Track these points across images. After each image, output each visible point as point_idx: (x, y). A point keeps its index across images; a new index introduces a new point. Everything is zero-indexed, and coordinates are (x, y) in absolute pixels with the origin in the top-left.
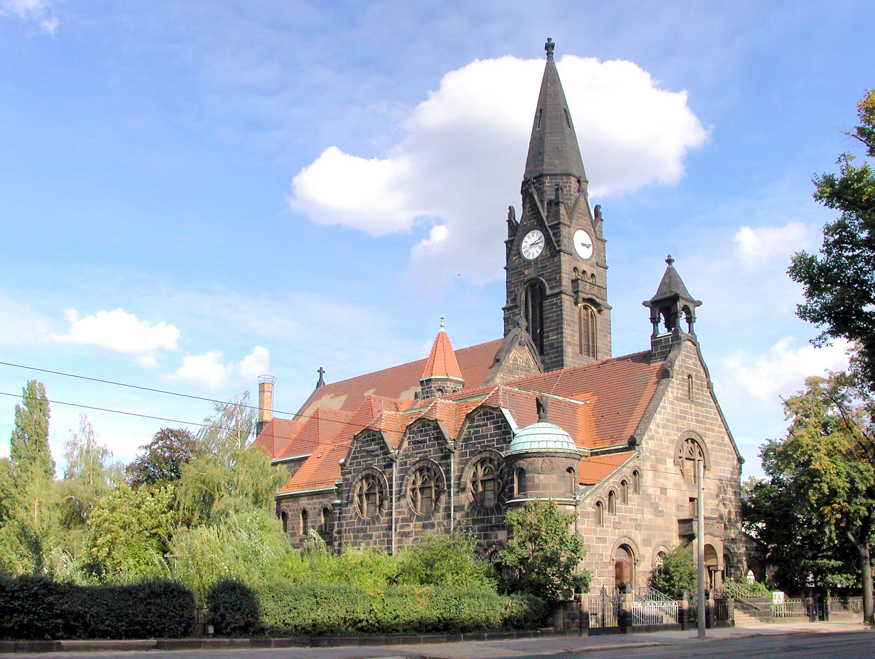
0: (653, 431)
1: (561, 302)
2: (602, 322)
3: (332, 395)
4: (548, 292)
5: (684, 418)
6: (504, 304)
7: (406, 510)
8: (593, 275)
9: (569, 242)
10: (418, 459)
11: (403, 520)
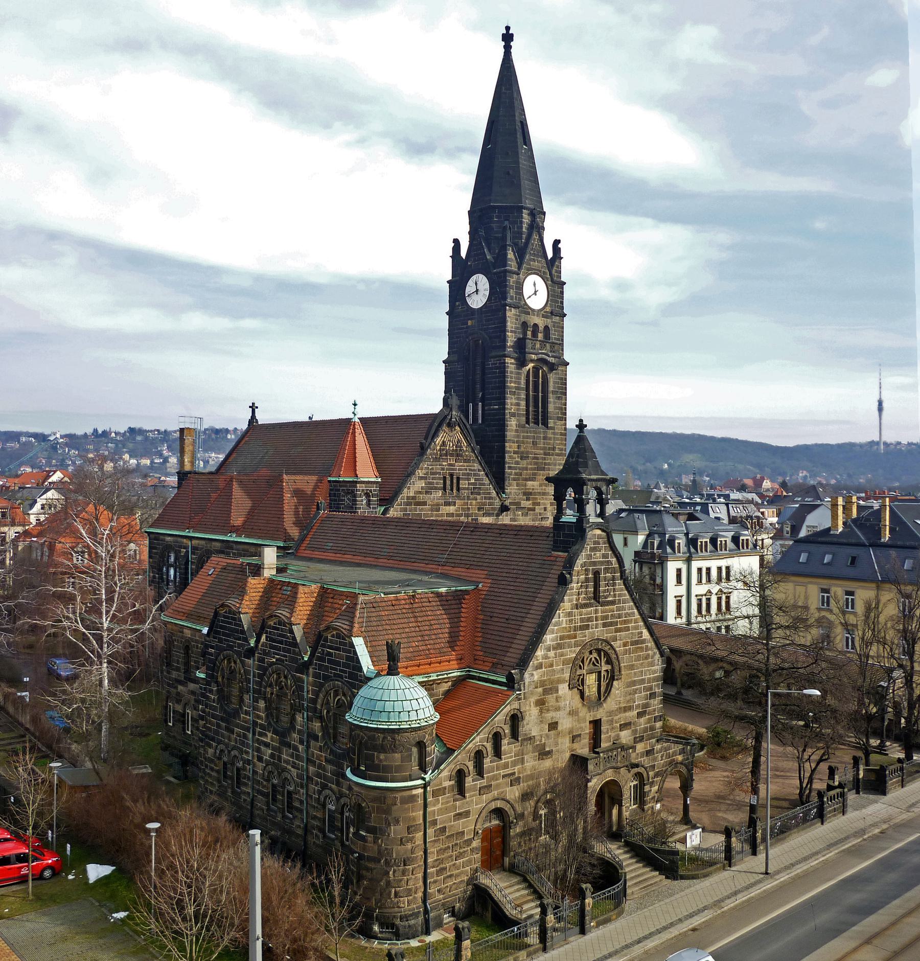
0: (539, 658)
1: (504, 367)
2: (555, 383)
5: (587, 627)
8: (546, 328)
9: (516, 293)
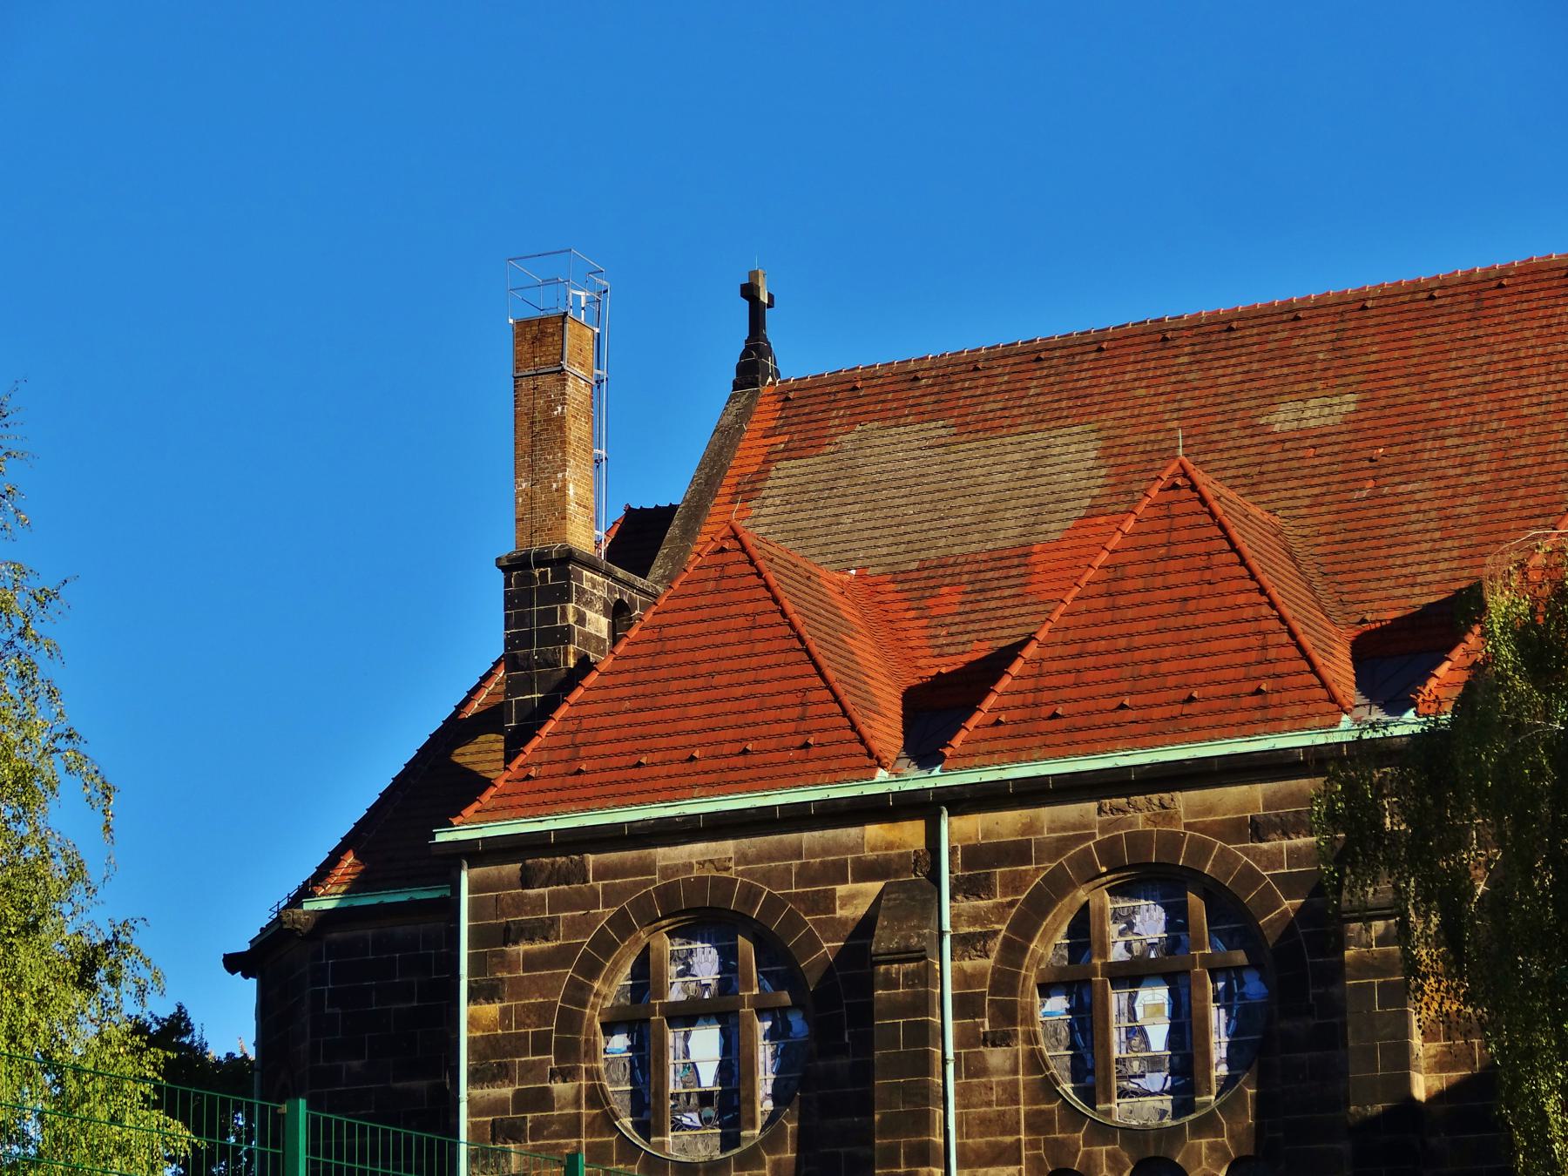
3: (936, 430)
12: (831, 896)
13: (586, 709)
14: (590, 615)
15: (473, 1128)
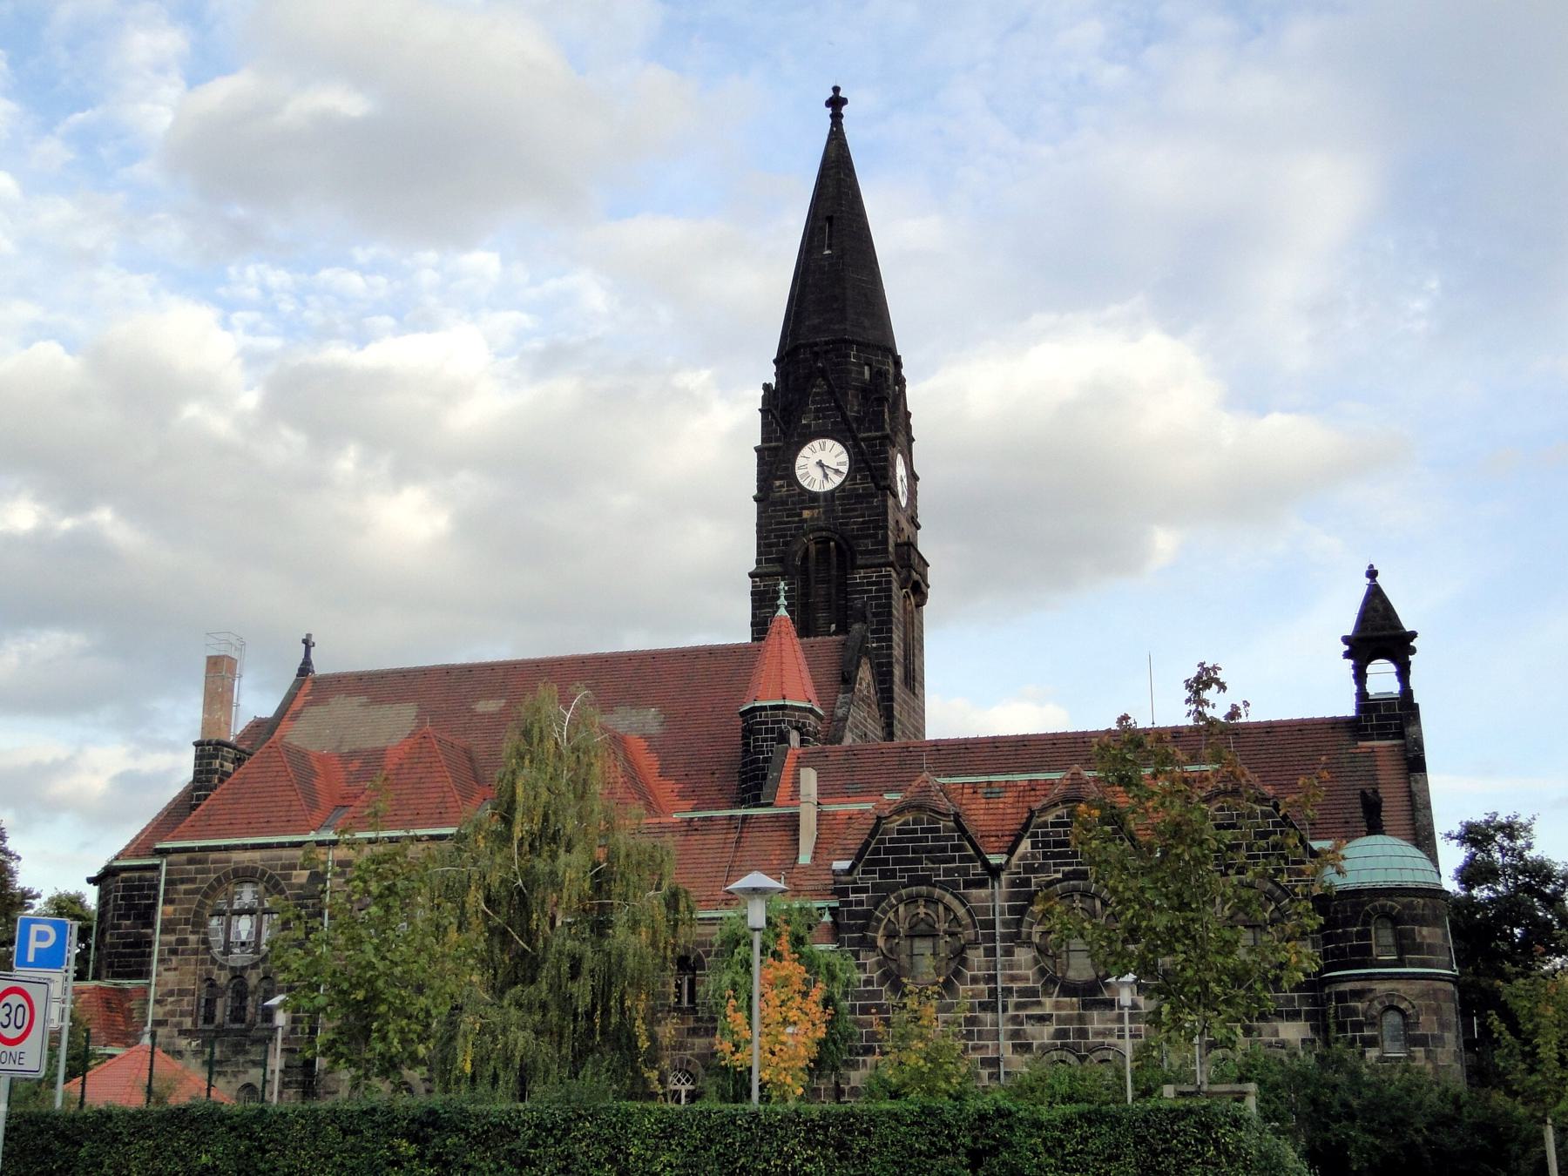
1: (890, 582)
3: (364, 699)
4: (860, 561)
6: (753, 567)
7: (1030, 973)
10: (1059, 876)
11: (1023, 992)
12: (291, 875)
13: (214, 802)
14: (225, 764)
15: (160, 952)
